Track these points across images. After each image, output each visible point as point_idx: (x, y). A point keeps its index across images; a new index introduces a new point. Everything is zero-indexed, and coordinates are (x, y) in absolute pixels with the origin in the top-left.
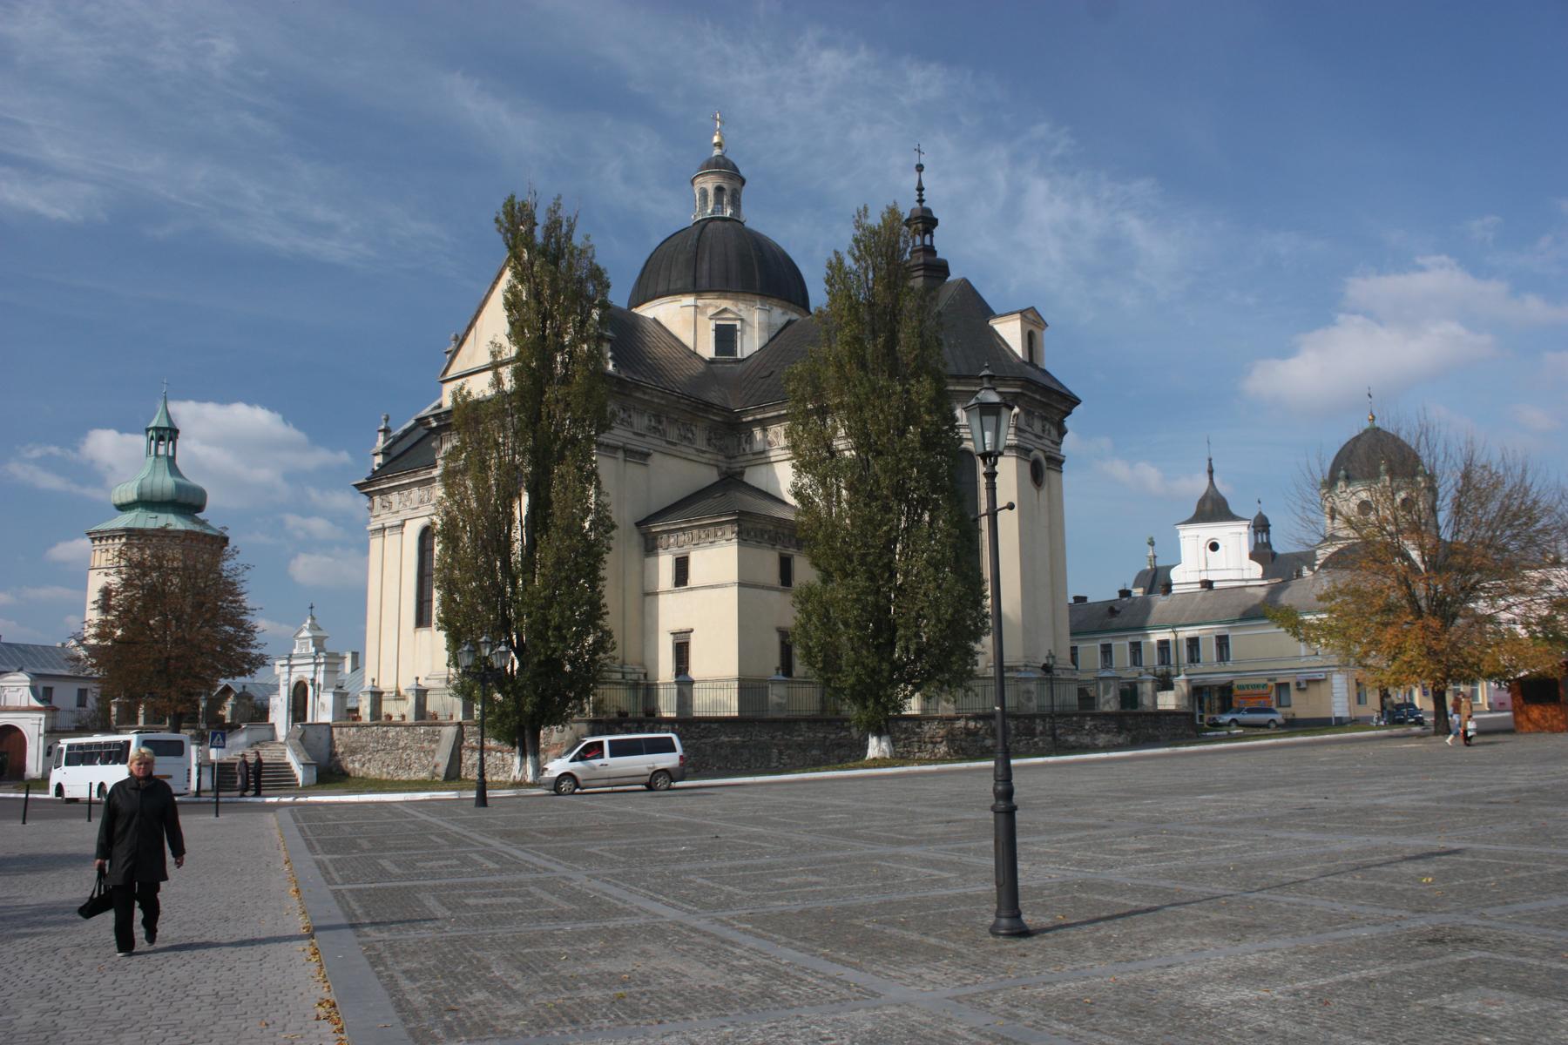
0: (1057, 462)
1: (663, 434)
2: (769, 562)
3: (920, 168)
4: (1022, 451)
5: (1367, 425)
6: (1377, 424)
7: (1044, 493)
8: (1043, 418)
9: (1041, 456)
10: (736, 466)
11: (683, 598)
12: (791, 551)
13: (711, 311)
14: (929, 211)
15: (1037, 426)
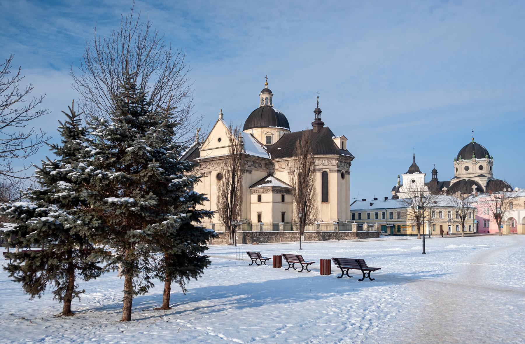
0: (348, 173)
1: (255, 166)
2: (279, 196)
3: (318, 97)
4: (338, 171)
5: (471, 141)
6: (475, 141)
7: (344, 180)
8: (345, 162)
9: (344, 171)
10: (271, 172)
11: (260, 204)
12: (284, 194)
13: (265, 132)
14: (319, 109)
15: (343, 164)
